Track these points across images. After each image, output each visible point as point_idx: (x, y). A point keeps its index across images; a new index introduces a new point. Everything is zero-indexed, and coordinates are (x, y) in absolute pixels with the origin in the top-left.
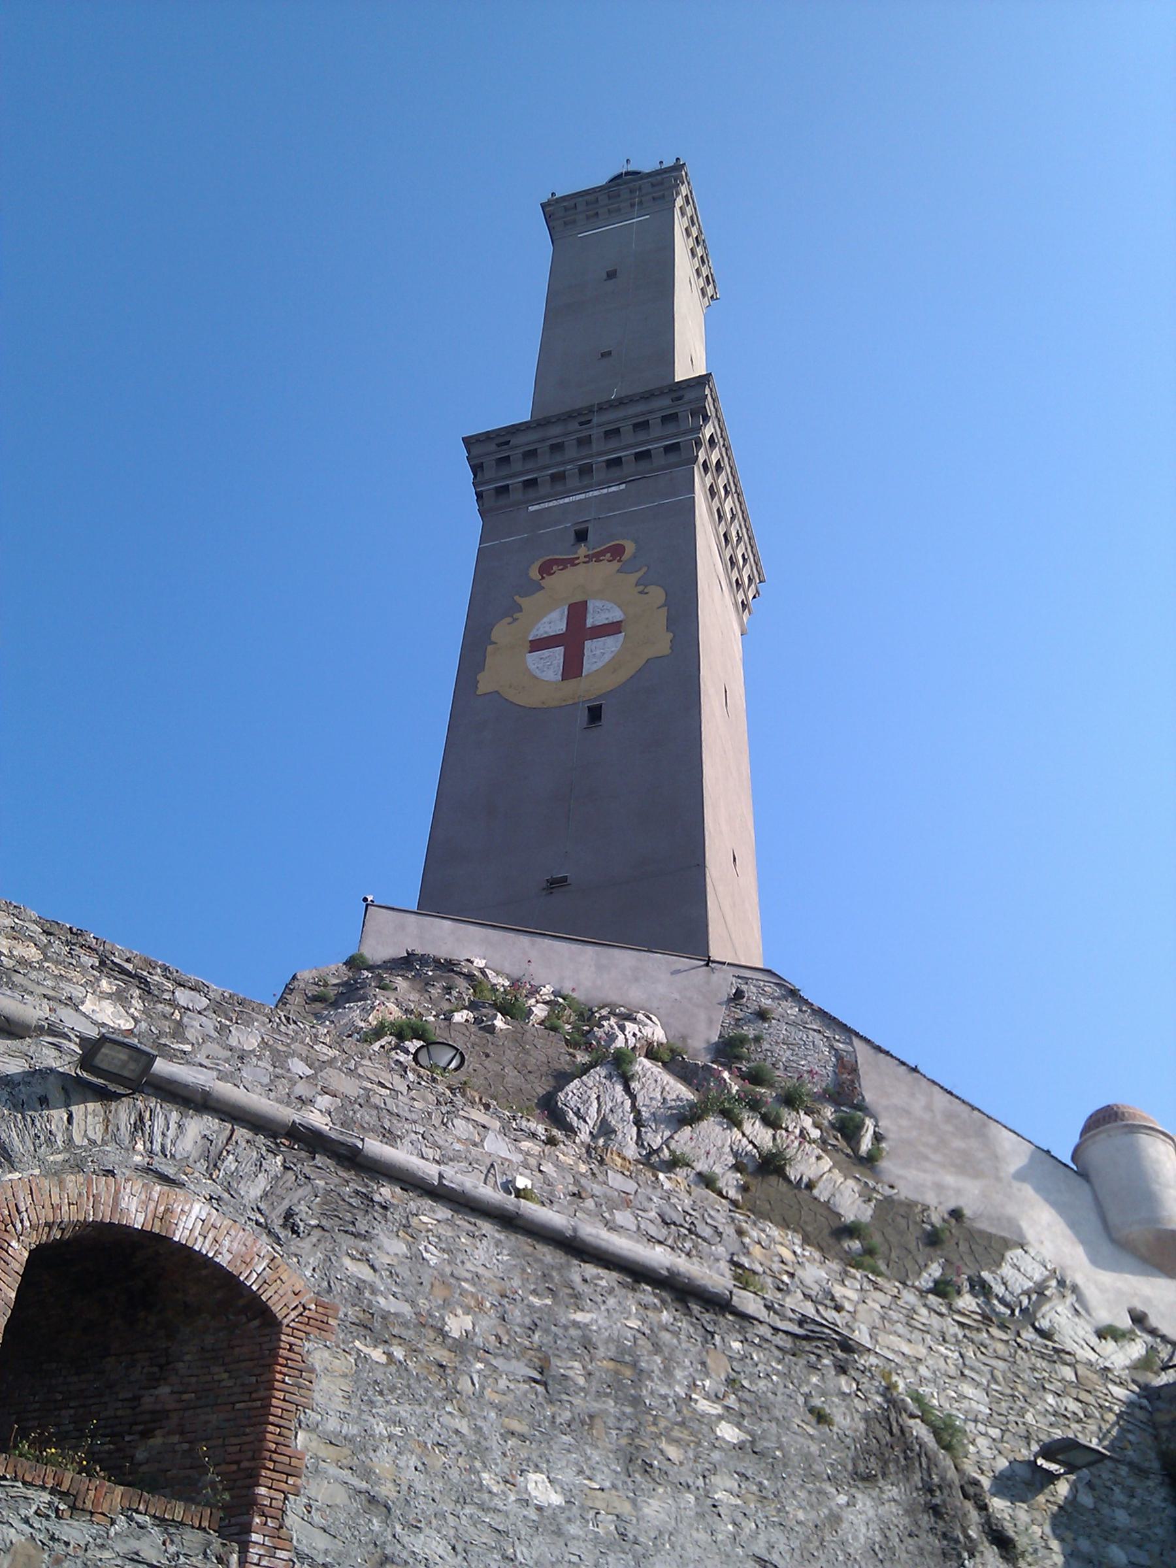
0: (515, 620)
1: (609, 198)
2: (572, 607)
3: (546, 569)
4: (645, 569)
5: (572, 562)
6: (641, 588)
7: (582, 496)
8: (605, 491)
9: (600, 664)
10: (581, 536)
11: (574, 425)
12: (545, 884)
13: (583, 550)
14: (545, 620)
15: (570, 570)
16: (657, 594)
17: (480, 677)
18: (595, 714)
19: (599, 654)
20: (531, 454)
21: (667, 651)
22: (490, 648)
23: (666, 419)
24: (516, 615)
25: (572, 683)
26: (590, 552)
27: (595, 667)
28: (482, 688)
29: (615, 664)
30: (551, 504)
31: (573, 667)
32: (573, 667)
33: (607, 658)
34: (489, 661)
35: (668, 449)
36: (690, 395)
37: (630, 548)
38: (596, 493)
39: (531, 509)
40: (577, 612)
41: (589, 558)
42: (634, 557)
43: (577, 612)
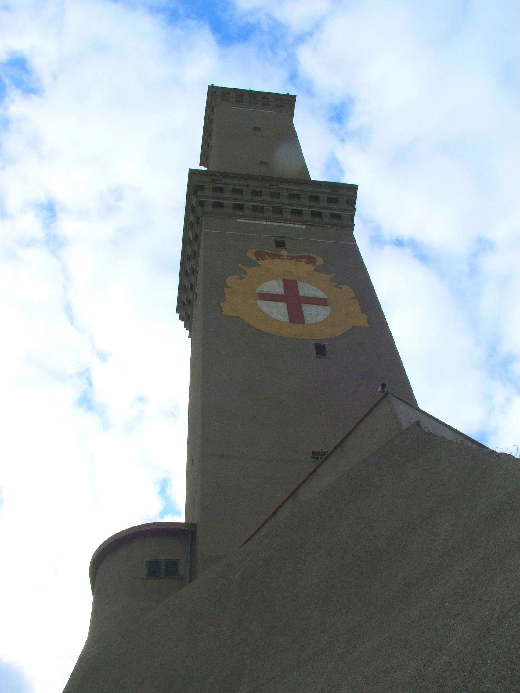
0: (242, 278)
3: (260, 255)
5: (279, 257)
6: (336, 284)
7: (276, 224)
8: (292, 225)
9: (318, 320)
10: (280, 244)
11: (267, 185)
12: (311, 455)
13: (284, 252)
14: (266, 284)
15: (276, 262)
16: (347, 292)
17: (222, 304)
21: (368, 326)
22: (226, 289)
23: (330, 200)
24: (243, 276)
26: (291, 255)
31: (296, 316)
32: (296, 316)
33: (321, 318)
35: (334, 216)
37: (320, 261)
40: (291, 286)
41: (291, 258)
43: (291, 286)
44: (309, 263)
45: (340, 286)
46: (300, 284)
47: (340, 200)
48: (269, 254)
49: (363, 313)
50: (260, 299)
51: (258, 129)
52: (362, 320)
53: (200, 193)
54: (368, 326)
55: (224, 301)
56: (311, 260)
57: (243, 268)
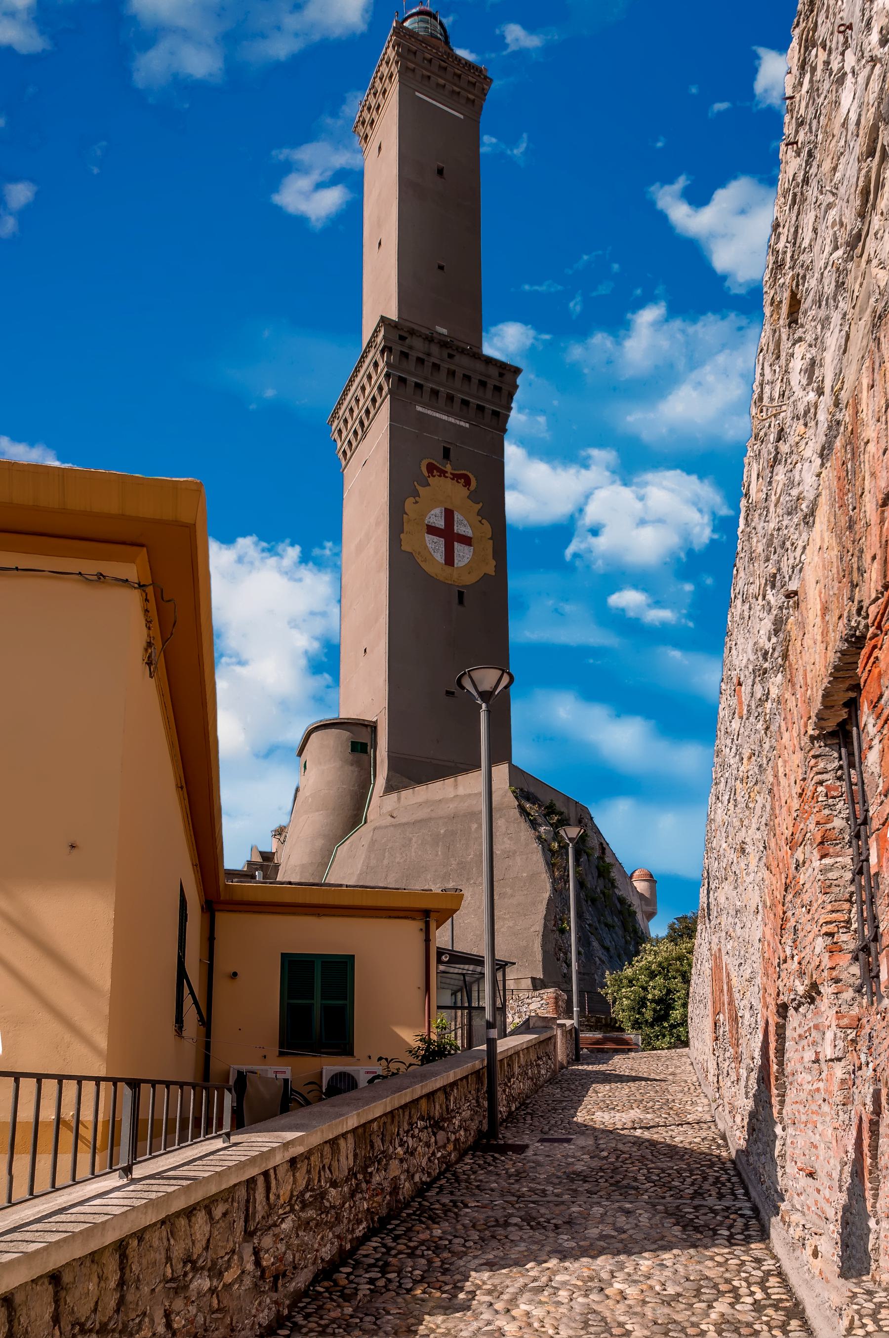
0: (416, 502)
1: (440, 66)
4: (481, 504)
8: (458, 422)
14: (432, 512)
16: (487, 528)
17: (402, 536)
18: (461, 595)
19: (463, 554)
20: (420, 361)
21: (494, 574)
24: (417, 498)
25: (448, 569)
27: (461, 564)
29: (469, 568)
30: (429, 412)
31: (449, 559)
32: (449, 559)
33: (466, 561)
34: (406, 528)
36: (508, 376)
38: (452, 420)
39: (419, 409)
42: (475, 491)
44: (465, 486)
45: (484, 521)
46: (457, 516)
49: (494, 558)
50: (428, 533)
51: (440, 172)
52: (490, 568)
54: (494, 574)
55: (403, 532)
56: (467, 483)
57: (418, 488)
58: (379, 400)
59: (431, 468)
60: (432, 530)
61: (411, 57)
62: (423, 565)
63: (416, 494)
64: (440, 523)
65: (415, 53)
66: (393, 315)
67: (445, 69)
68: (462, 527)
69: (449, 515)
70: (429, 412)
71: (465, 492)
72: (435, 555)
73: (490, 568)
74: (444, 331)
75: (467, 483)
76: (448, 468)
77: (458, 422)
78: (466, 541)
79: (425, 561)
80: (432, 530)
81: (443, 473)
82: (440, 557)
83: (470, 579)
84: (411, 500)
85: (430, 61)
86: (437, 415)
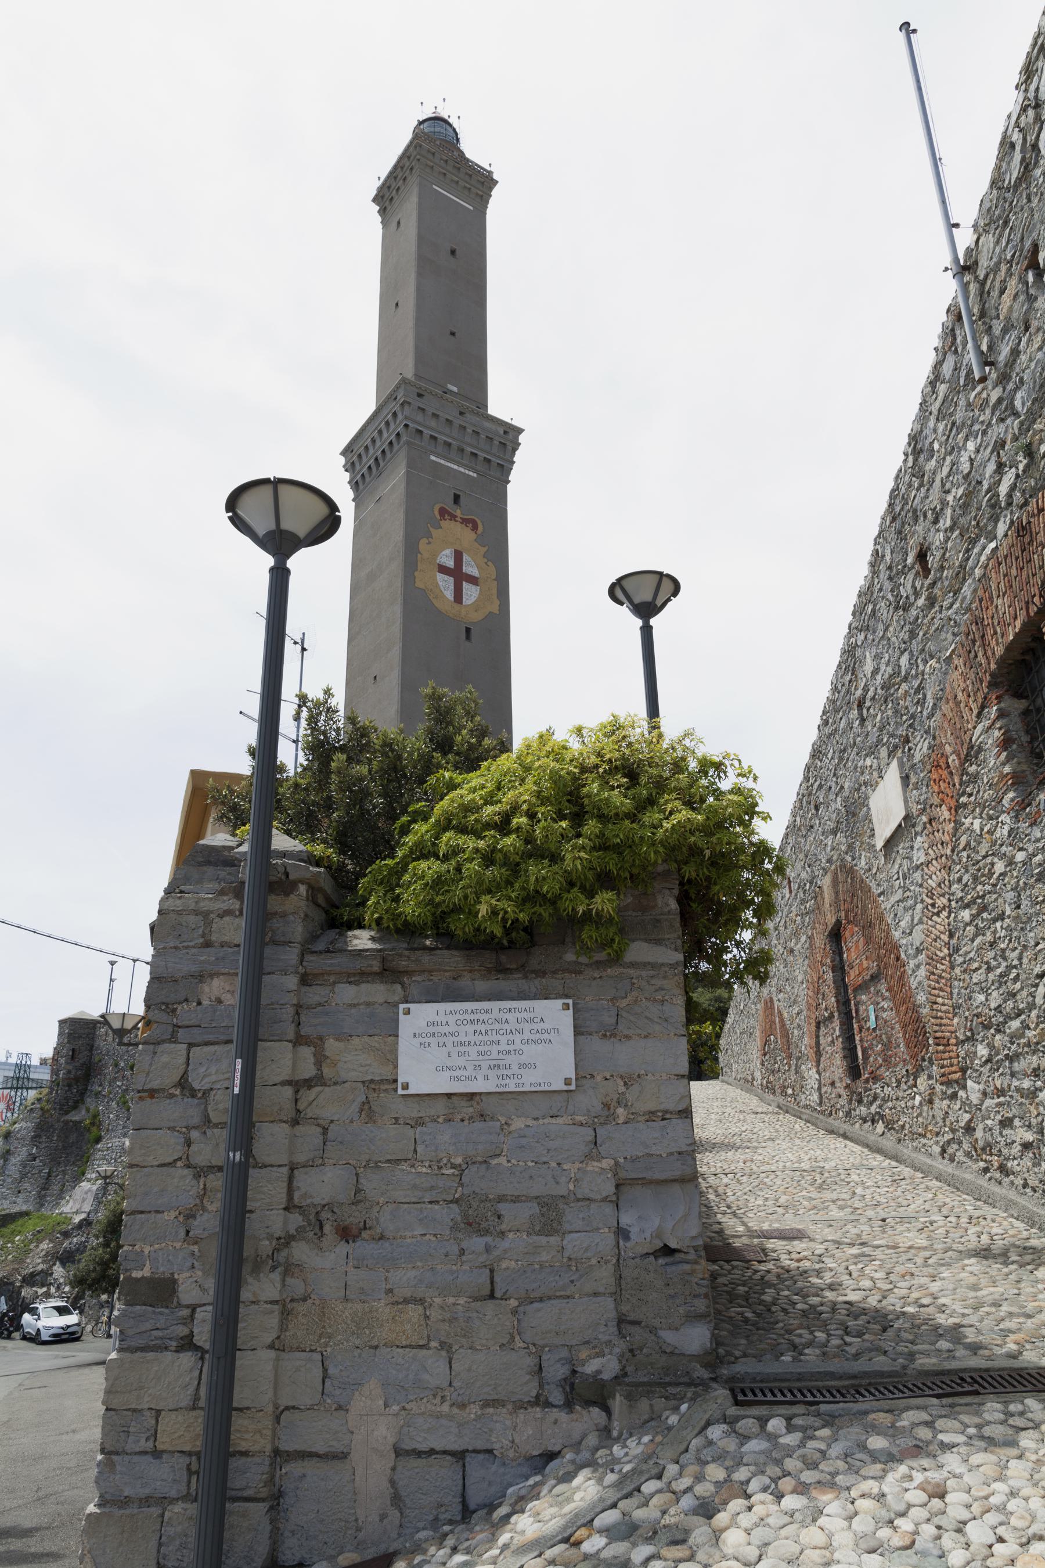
0: (429, 543)
2: (456, 551)
8: (467, 472)
16: (492, 569)
17: (416, 574)
18: (468, 631)
20: (435, 416)
25: (457, 606)
27: (469, 602)
28: (419, 584)
29: (476, 606)
30: (442, 462)
33: (473, 599)
38: (462, 470)
39: (433, 458)
41: (465, 521)
45: (490, 563)
46: (466, 558)
47: (507, 438)
48: (450, 514)
51: (453, 252)
52: (495, 608)
53: (406, 407)
58: (396, 447)
59: (443, 512)
60: (443, 569)
61: (430, 156)
62: (434, 601)
63: (429, 536)
64: (450, 563)
65: (434, 154)
66: (409, 374)
67: (459, 169)
68: (470, 568)
69: (458, 556)
70: (442, 462)
71: (472, 536)
72: (445, 593)
73: (495, 608)
74: (455, 389)
75: (475, 528)
76: (458, 513)
77: (467, 472)
78: (473, 580)
79: (436, 597)
80: (443, 569)
81: (453, 517)
82: (449, 594)
83: (476, 617)
84: (424, 541)
85: (446, 161)
86: (449, 465)
